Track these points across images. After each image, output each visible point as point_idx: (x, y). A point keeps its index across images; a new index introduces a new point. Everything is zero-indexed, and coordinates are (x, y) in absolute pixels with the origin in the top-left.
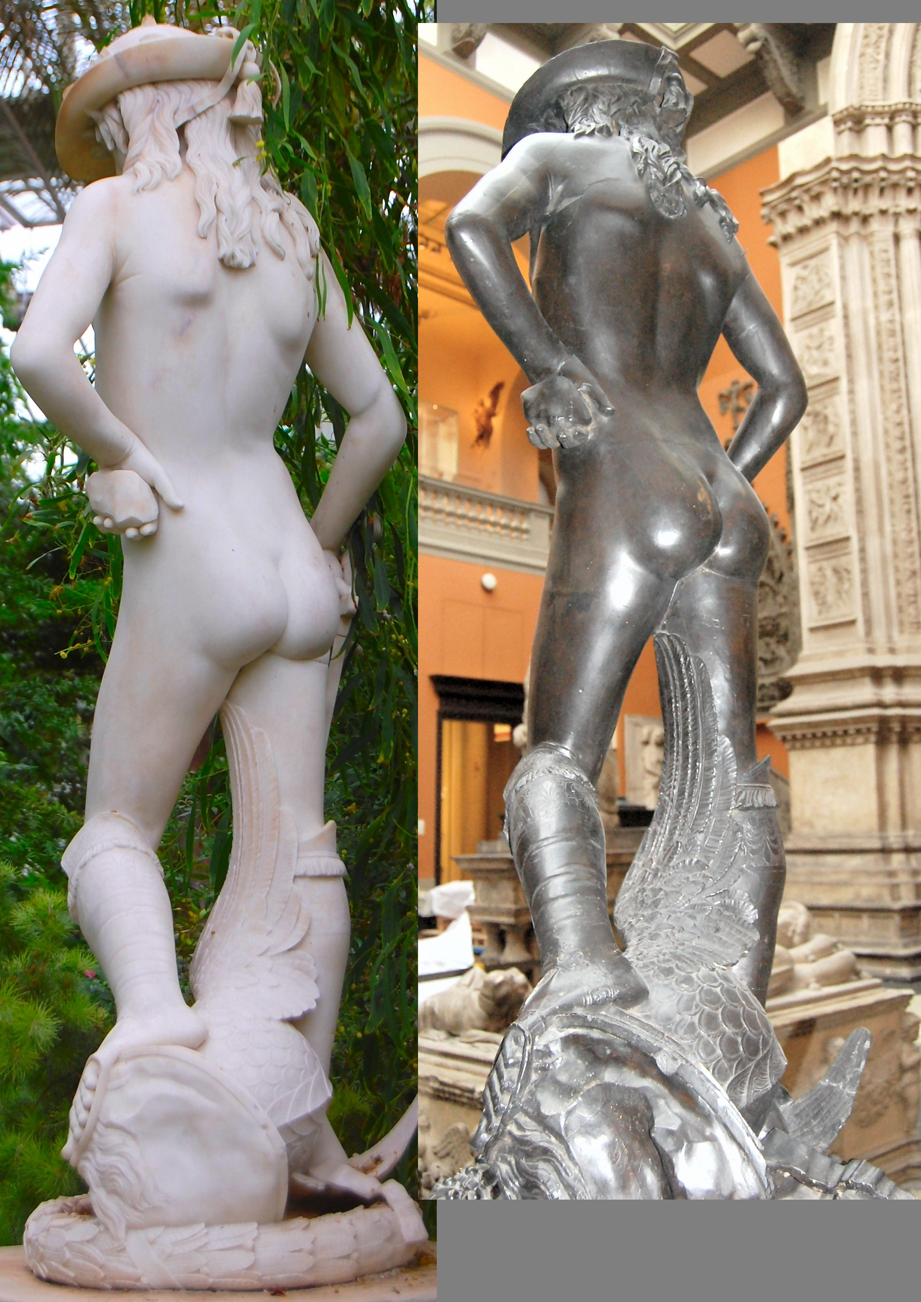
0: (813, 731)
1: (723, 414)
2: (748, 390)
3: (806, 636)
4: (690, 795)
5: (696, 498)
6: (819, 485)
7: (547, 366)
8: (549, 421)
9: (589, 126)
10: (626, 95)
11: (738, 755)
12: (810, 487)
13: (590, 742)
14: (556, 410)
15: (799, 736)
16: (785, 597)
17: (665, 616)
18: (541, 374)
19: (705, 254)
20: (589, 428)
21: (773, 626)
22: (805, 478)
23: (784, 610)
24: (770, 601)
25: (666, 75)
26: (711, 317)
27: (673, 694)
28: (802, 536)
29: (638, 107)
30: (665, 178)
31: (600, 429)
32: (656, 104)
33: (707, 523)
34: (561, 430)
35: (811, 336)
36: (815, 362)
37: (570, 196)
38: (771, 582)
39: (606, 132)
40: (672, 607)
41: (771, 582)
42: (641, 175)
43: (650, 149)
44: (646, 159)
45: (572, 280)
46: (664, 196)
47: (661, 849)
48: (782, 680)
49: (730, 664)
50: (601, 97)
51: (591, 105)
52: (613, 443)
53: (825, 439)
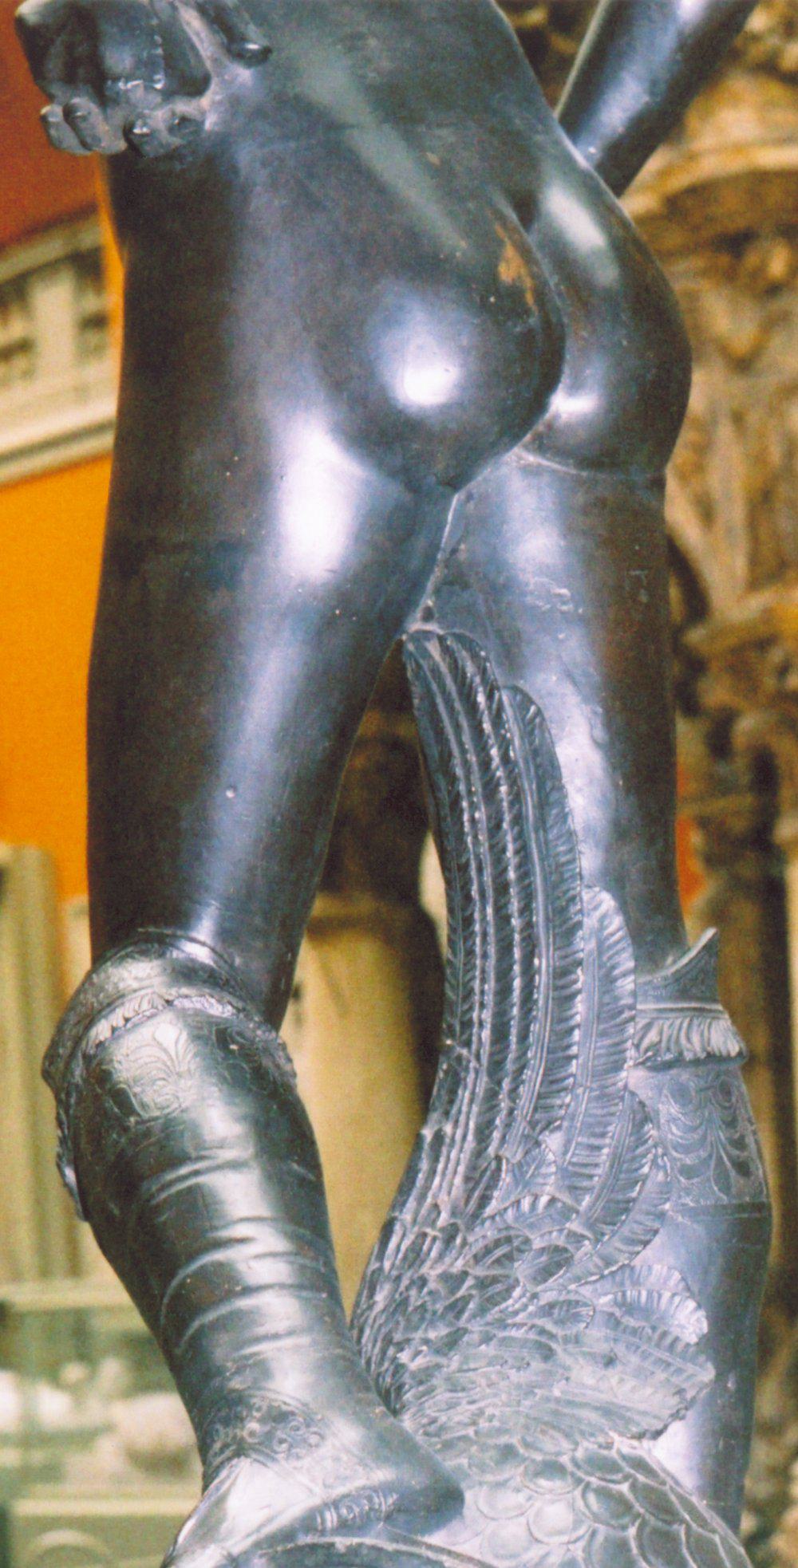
4: (524, 1037)
11: (636, 933)
13: (258, 921)
14: (119, 58)
17: (430, 585)
20: (205, 101)
31: (234, 103)
47: (458, 1180)
49: (604, 703)
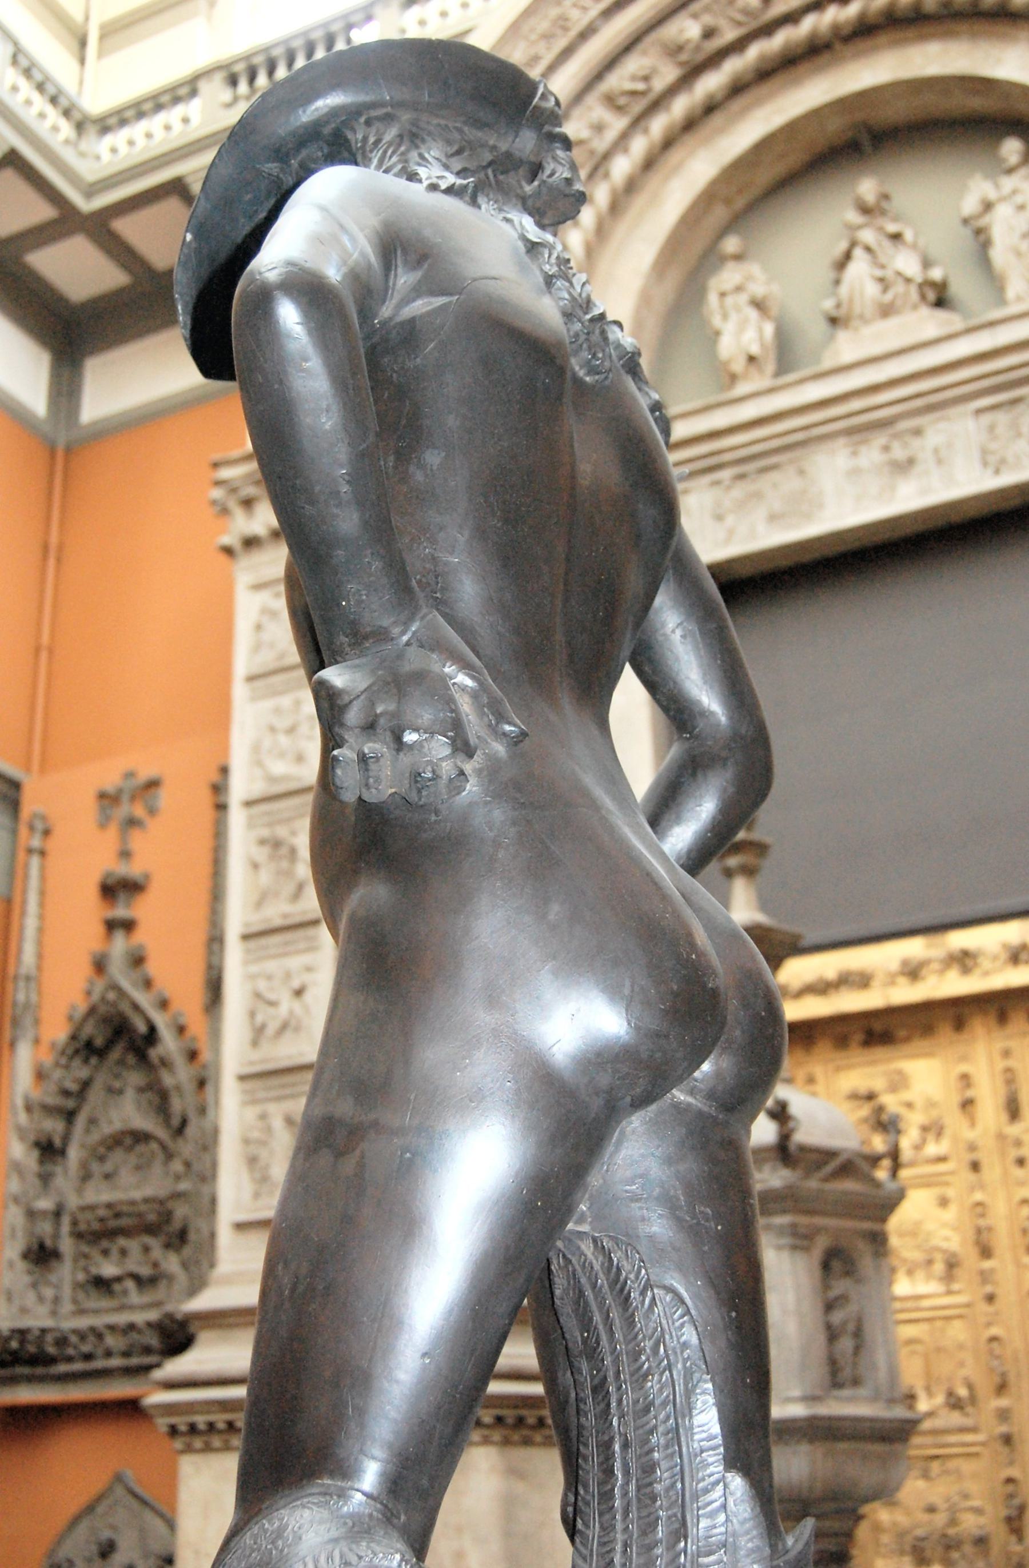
0: (228, 1416)
1: (103, 825)
2: (153, 790)
3: (225, 1235)
6: (271, 966)
12: (254, 969)
15: (202, 1427)
16: (188, 1165)
18: (366, 637)
21: (159, 1214)
22: (248, 951)
23: (184, 1186)
24: (157, 1168)
28: (234, 1051)
35: (278, 711)
36: (282, 755)
37: (433, 293)
38: (161, 1133)
41: (161, 1133)
48: (170, 1316)
53: (289, 888)
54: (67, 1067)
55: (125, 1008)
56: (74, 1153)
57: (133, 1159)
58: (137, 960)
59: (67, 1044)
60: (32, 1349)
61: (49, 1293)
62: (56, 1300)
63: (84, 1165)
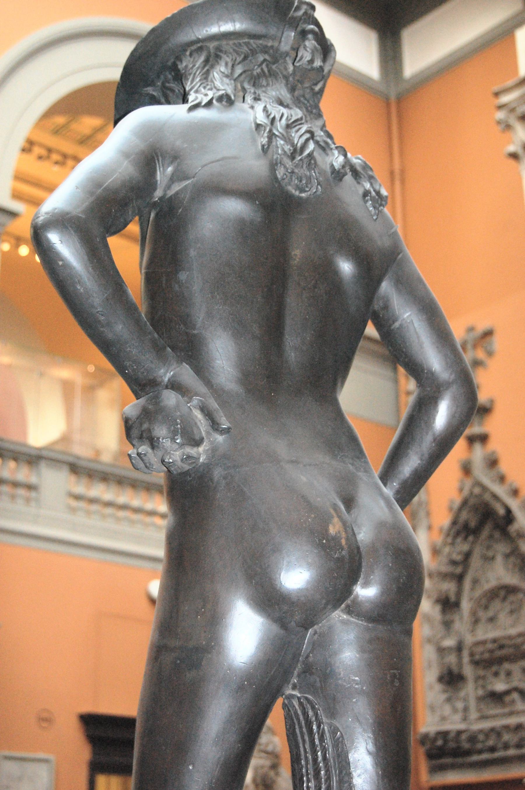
2: (488, 339)
5: (327, 530)
7: (151, 377)
8: (153, 443)
9: (206, 95)
10: (254, 52)
17: (296, 673)
19: (347, 236)
20: (201, 449)
25: (299, 29)
26: (353, 309)
27: (304, 770)
29: (267, 66)
30: (295, 150)
31: (214, 450)
32: (289, 61)
33: (340, 560)
34: (167, 452)
39: (227, 101)
40: (303, 662)
42: (265, 150)
43: (278, 117)
44: (270, 131)
45: (183, 276)
46: (293, 172)
49: (374, 733)
50: (224, 56)
51: (212, 67)
52: (228, 467)
54: (453, 544)
55: (487, 497)
56: (466, 605)
57: (507, 607)
58: (493, 463)
59: (450, 529)
60: (452, 745)
61: (460, 705)
62: (466, 709)
63: (474, 613)
